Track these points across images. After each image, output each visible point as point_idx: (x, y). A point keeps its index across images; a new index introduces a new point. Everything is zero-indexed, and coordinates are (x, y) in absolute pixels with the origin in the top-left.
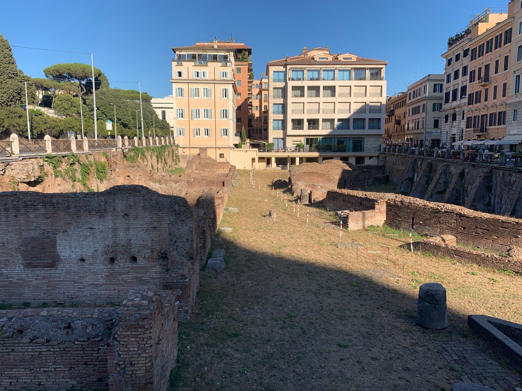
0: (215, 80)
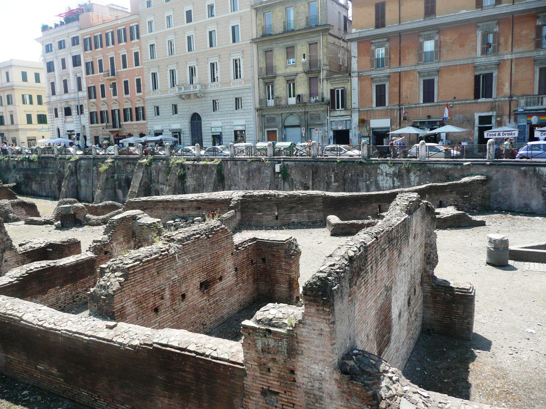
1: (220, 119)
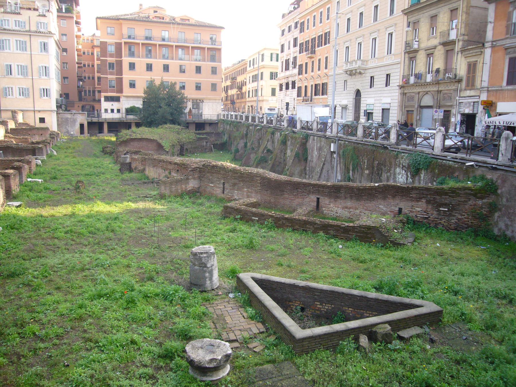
0: (29, 31)
1: (373, 96)
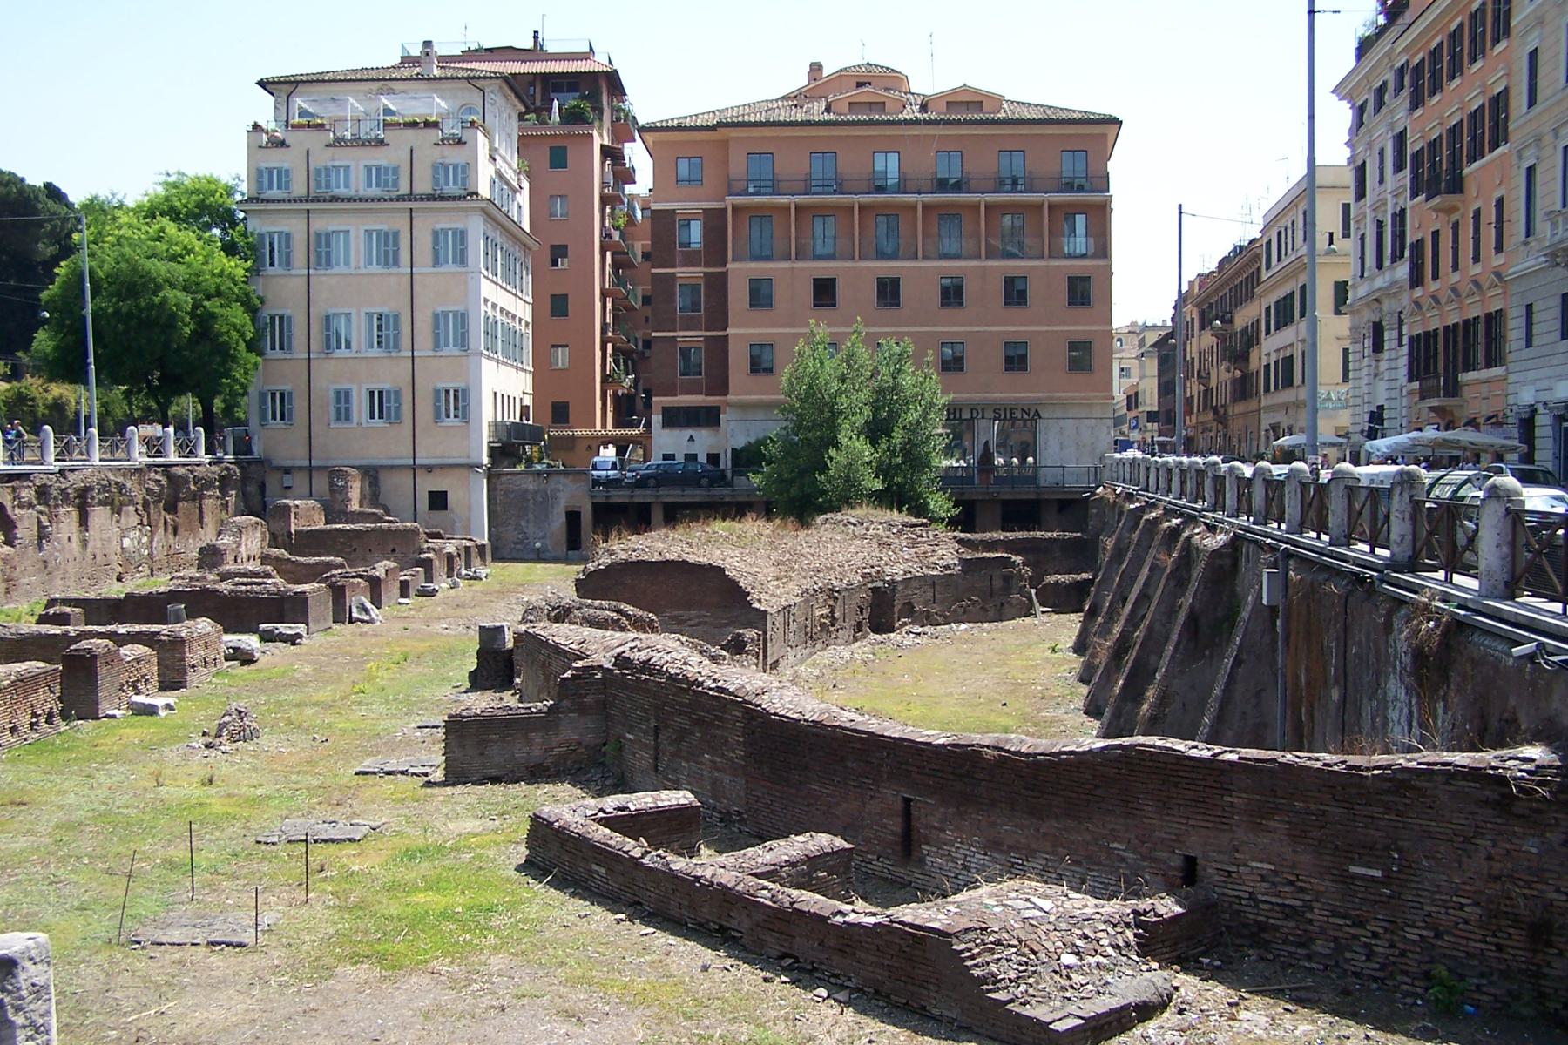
0: (410, 197)
